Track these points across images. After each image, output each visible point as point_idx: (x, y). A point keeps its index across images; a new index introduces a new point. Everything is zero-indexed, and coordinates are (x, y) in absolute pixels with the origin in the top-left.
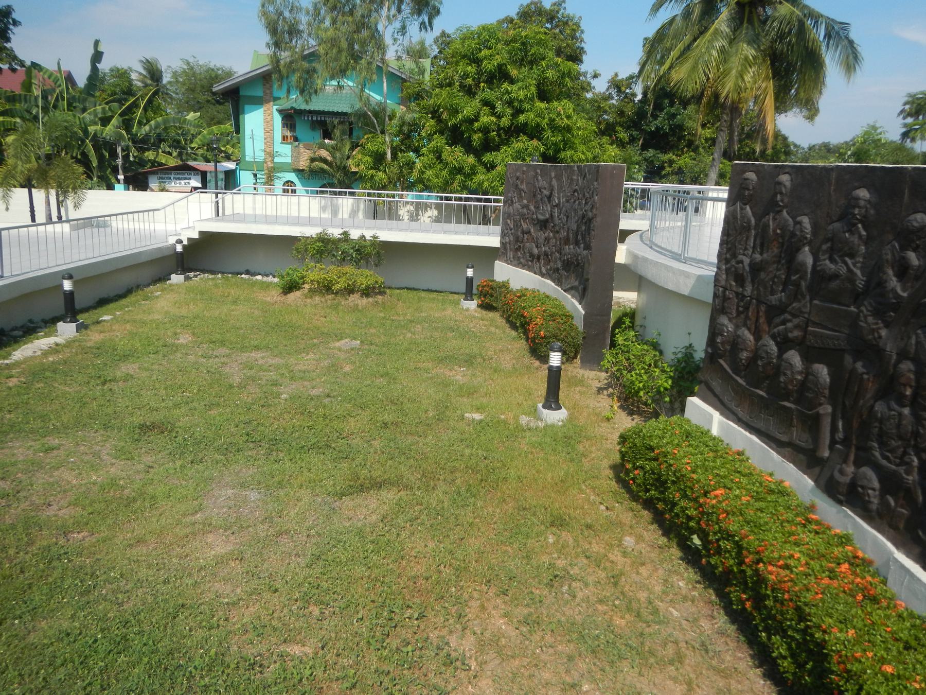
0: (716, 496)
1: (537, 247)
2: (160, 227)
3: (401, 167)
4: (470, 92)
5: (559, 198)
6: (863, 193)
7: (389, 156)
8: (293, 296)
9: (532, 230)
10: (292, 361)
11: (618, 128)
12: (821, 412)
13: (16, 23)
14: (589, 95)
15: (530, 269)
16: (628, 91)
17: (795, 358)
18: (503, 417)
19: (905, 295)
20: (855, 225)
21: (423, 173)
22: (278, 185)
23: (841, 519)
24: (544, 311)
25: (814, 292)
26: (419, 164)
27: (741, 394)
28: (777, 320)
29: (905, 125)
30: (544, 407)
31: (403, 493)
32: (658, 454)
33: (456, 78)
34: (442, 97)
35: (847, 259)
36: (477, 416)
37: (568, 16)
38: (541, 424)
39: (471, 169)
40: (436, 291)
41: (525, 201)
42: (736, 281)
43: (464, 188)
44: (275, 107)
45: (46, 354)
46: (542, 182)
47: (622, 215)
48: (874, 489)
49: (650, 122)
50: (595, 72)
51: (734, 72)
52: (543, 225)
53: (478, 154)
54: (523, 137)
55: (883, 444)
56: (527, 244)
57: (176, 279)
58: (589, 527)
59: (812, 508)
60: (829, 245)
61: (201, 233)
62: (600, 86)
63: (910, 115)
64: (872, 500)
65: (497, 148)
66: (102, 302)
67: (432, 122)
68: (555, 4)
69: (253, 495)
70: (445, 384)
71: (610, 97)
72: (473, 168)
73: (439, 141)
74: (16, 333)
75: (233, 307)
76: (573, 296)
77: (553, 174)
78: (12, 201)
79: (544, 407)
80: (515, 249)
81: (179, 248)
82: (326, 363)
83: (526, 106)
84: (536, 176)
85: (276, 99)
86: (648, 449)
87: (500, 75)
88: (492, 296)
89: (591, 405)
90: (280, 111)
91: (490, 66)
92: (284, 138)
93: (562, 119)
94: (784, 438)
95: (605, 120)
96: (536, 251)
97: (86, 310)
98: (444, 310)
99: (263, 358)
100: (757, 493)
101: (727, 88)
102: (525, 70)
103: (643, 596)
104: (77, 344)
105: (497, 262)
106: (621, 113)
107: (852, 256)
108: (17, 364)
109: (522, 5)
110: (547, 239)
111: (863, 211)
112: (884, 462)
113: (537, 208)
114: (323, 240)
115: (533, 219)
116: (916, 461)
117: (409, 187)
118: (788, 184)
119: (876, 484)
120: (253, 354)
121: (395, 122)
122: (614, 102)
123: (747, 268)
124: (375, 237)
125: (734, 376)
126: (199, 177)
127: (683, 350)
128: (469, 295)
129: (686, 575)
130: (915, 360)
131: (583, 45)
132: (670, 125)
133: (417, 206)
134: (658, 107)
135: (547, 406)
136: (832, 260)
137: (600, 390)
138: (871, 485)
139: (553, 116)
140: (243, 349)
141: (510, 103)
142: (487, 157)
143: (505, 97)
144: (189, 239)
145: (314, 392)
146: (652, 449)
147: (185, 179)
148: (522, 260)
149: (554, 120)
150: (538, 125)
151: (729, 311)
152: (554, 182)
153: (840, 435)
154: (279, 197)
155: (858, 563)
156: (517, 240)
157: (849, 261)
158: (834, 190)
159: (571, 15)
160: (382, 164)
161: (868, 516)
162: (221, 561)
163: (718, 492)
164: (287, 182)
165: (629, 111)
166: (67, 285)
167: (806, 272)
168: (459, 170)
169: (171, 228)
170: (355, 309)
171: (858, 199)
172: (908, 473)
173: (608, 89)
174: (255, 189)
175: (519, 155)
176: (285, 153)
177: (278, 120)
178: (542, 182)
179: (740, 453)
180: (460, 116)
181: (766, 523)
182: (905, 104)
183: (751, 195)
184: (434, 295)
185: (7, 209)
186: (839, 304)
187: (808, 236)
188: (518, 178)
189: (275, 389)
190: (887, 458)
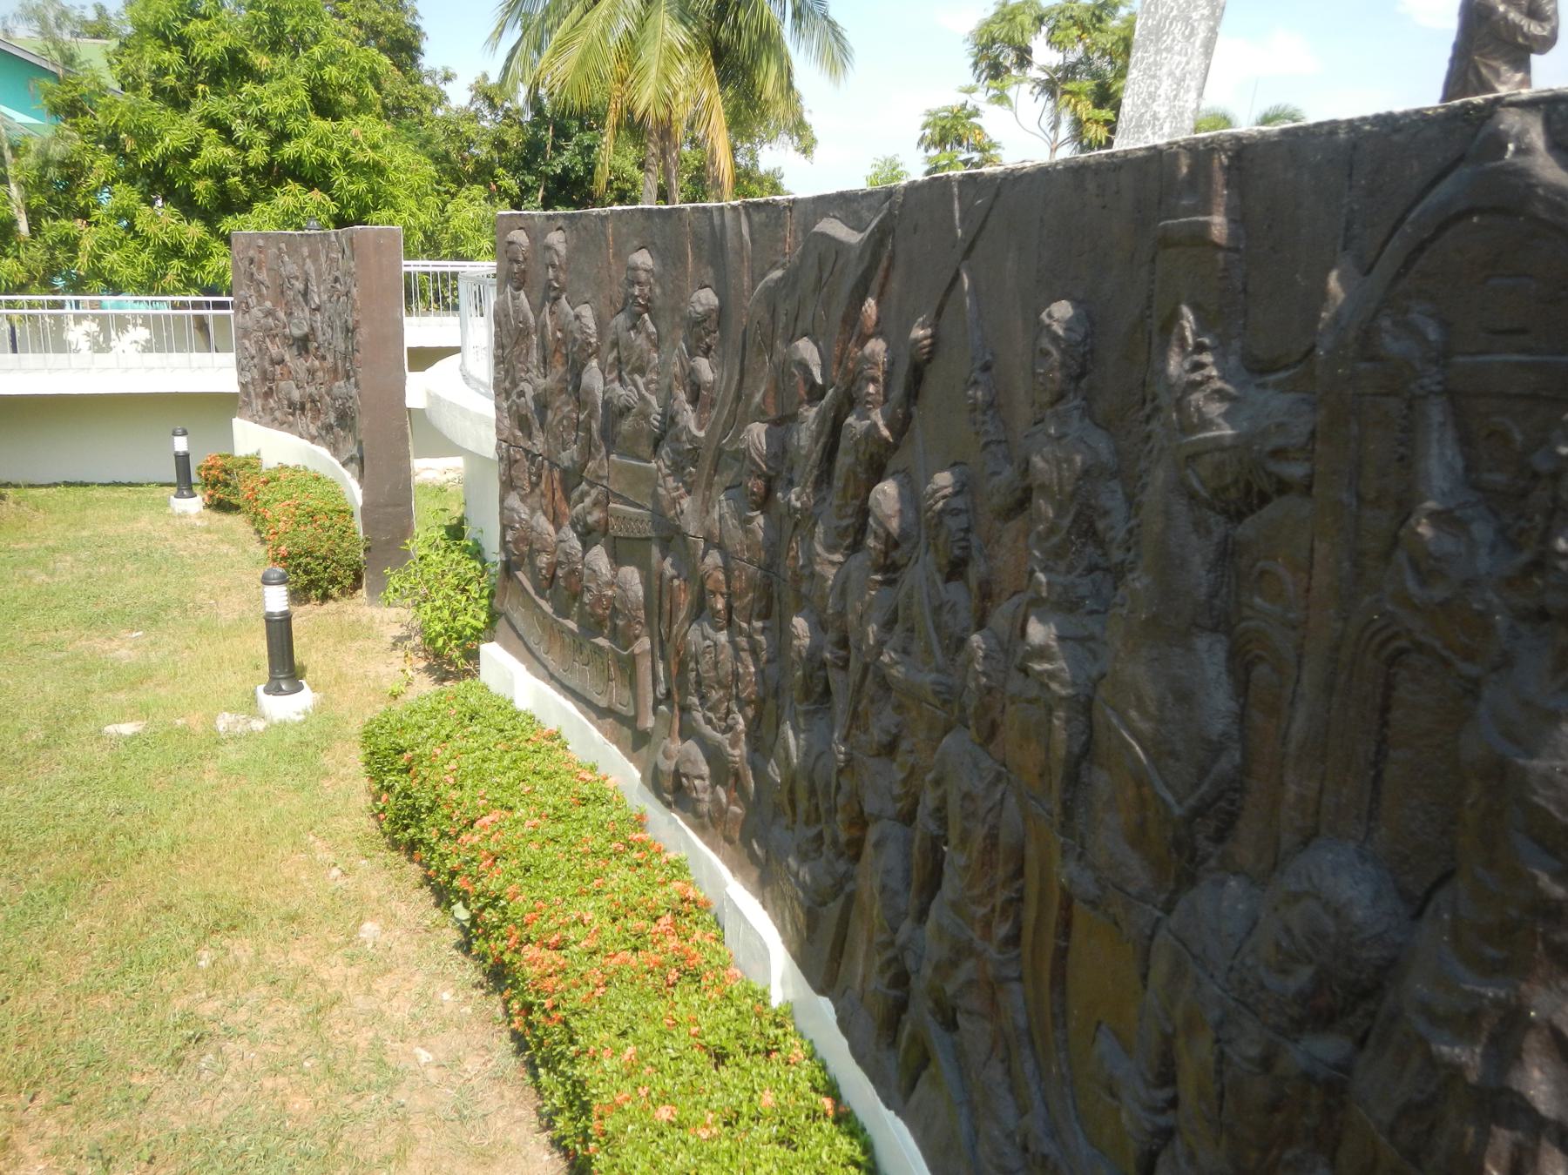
0: (484, 827)
3: (51, 248)
4: (178, 102)
6: (643, 259)
7: (23, 226)
9: (287, 358)
11: (500, 171)
12: (637, 651)
14: (440, 113)
16: (507, 105)
17: (599, 558)
18: (179, 722)
19: (702, 434)
20: (640, 315)
21: (99, 258)
23: (675, 835)
25: (610, 437)
26: (87, 243)
27: (552, 631)
28: (575, 495)
29: (929, 159)
30: (267, 691)
32: (411, 760)
33: (144, 74)
34: (121, 107)
35: (637, 377)
36: (127, 729)
38: (258, 725)
39: (198, 247)
40: (130, 484)
41: (268, 304)
42: (521, 430)
43: (189, 283)
46: (291, 268)
47: (407, 320)
48: (701, 778)
50: (445, 69)
51: (654, 70)
52: (303, 344)
53: (209, 218)
54: (293, 186)
55: (703, 698)
56: (282, 383)
59: (640, 822)
60: (615, 353)
62: (459, 96)
63: (933, 143)
64: (701, 796)
65: (246, 207)
67: (109, 159)
71: (476, 117)
72: (201, 245)
73: (126, 195)
77: (305, 251)
79: (267, 691)
80: (264, 394)
83: (293, 125)
84: (279, 256)
87: (232, 70)
88: (227, 485)
89: (372, 674)
91: (209, 50)
93: (362, 150)
94: (603, 703)
95: (473, 156)
98: (135, 519)
100: (555, 808)
101: (645, 97)
102: (283, 59)
103: (363, 1038)
105: (238, 423)
106: (500, 145)
107: (641, 371)
111: (646, 290)
112: (708, 730)
113: (290, 314)
115: (285, 337)
116: (741, 725)
118: (562, 249)
119: (705, 769)
121: (30, 160)
122: (485, 124)
123: (531, 405)
125: (537, 598)
128: (184, 484)
130: (720, 547)
131: (418, 22)
132: (586, 164)
133: (103, 321)
134: (562, 133)
135: (274, 689)
136: (621, 379)
137: (398, 642)
138: (696, 773)
139: (347, 146)
141: (261, 122)
142: (228, 224)
143: (252, 110)
148: (278, 414)
149: (347, 153)
150: (323, 163)
151: (519, 484)
153: (662, 689)
155: (688, 909)
156: (265, 377)
157: (640, 381)
158: (615, 255)
160: (9, 244)
161: (700, 829)
165: (513, 137)
167: (595, 404)
168: (176, 251)
171: (635, 268)
172: (734, 745)
173: (471, 103)
175: (290, 218)
179: (554, 736)
180: (159, 149)
181: (554, 864)
182: (925, 127)
183: (524, 272)
184: (122, 492)
186: (639, 458)
187: (593, 340)
188: (252, 261)
190: (709, 721)
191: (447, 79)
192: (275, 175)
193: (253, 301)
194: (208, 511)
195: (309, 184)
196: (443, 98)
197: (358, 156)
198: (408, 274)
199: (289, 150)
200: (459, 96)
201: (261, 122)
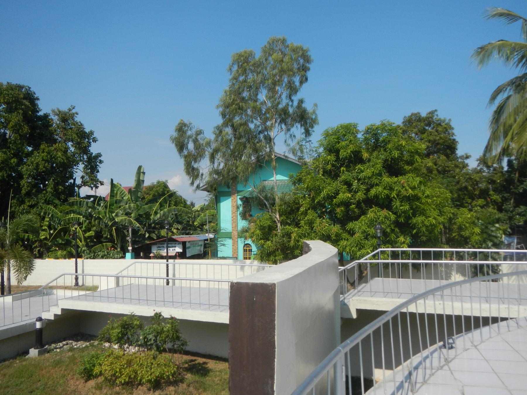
13: (101, 162)
21: (298, 241)
37: (440, 120)
39: (336, 236)
44: (239, 197)
49: (518, 186)
53: (343, 222)
62: (473, 164)
65: (357, 218)
68: (430, 113)
71: (481, 171)
72: (337, 235)
85: (239, 192)
91: (345, 153)
93: (406, 190)
106: (493, 182)
109: (405, 117)
126: (181, 246)
131: (454, 137)
139: (400, 188)
147: (173, 247)
149: (400, 191)
150: (388, 197)
159: (442, 118)
173: (478, 166)
191: (467, 157)
192: (370, 202)
195: (382, 207)
196: (465, 166)
197: (404, 193)
199: (373, 192)
200: (473, 164)
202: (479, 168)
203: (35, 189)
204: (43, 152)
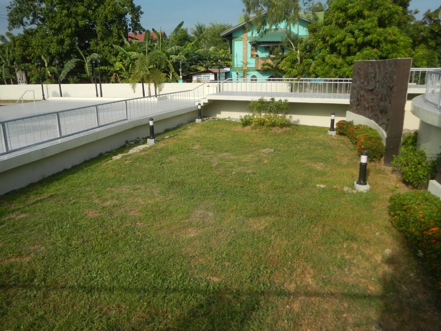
0: (433, 231)
1: (367, 103)
2: (192, 98)
3: (304, 66)
4: (342, 26)
5: (379, 78)
8: (248, 128)
9: (365, 95)
10: (242, 157)
13: (142, 13)
14: (412, 23)
15: (364, 115)
16: (435, 19)
18: (335, 187)
22: (249, 78)
24: (366, 136)
26: (313, 64)
30: (357, 183)
31: (277, 218)
32: (407, 208)
33: (334, 20)
36: (322, 186)
38: (355, 192)
41: (362, 80)
43: (336, 75)
45: (141, 151)
53: (344, 57)
54: (369, 48)
56: (363, 102)
57: (198, 121)
58: (367, 242)
61: (209, 100)
62: (419, 17)
65: (355, 54)
66: (167, 131)
69: (211, 214)
70: (311, 170)
71: (425, 23)
72: (342, 64)
74: (131, 143)
75: (220, 133)
76: (383, 128)
77: (377, 66)
78: (136, 89)
80: (357, 106)
81: (199, 107)
82: (257, 159)
83: (372, 31)
84: (368, 67)
86: (402, 205)
89: (385, 184)
90: (250, 43)
92: (252, 56)
95: (421, 35)
96: (367, 105)
97: (159, 134)
98: (319, 135)
99: (228, 156)
104: (153, 148)
108: (130, 155)
110: (373, 99)
114: (261, 102)
115: (366, 89)
117: (309, 75)
120: (224, 154)
121: (303, 44)
122: (427, 25)
124: (286, 100)
127: (436, 156)
129: (415, 271)
135: (359, 183)
139: (385, 35)
140: (221, 152)
141: (362, 30)
142: (349, 58)
143: (361, 27)
144: (204, 103)
145: (248, 172)
146: (403, 205)
148: (360, 110)
149: (387, 37)
152: (377, 70)
154: (248, 83)
156: (358, 100)
162: (191, 240)
163: (434, 229)
164: (253, 76)
166: (151, 123)
169: (196, 98)
170: (275, 134)
173: (423, 19)
174: (237, 80)
175: (366, 56)
176: (252, 63)
177: (249, 46)
178: (371, 70)
185: (134, 92)
189: (231, 169)
191: (416, 12)
193: (357, 80)
194: (337, 135)
195: (373, 47)
196: (413, 18)
197: (389, 38)
198: (412, 72)
199: (369, 37)
201: (362, 30)
202: (423, 21)
203: (108, 34)
204: (109, 5)
